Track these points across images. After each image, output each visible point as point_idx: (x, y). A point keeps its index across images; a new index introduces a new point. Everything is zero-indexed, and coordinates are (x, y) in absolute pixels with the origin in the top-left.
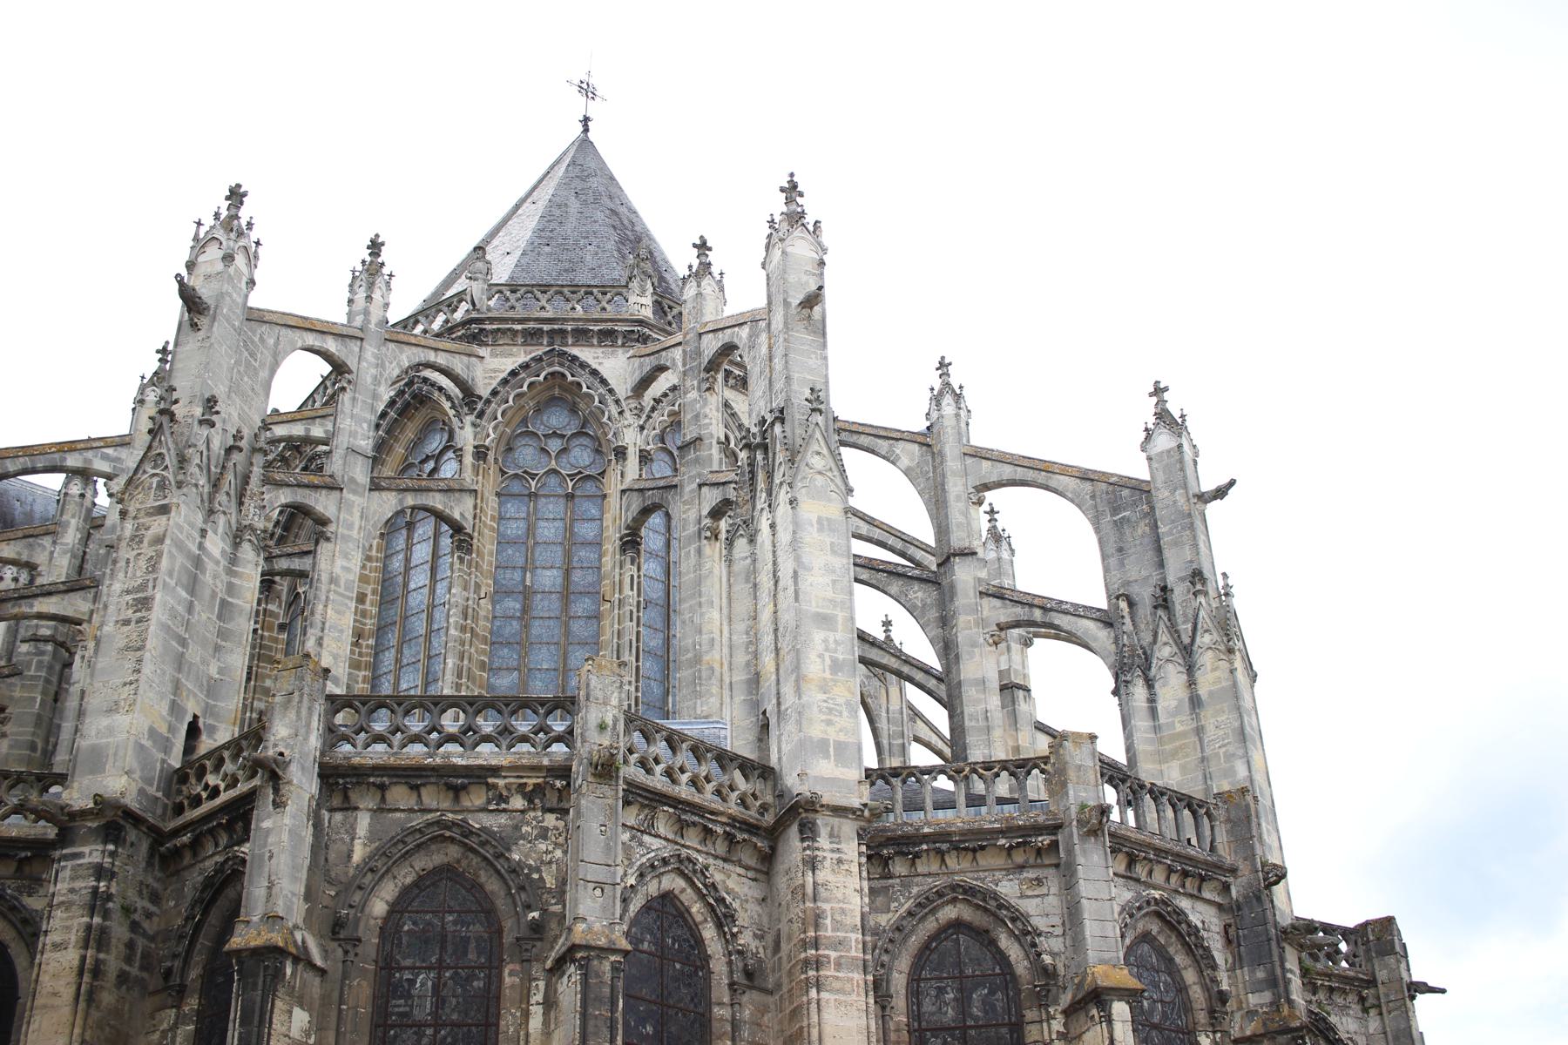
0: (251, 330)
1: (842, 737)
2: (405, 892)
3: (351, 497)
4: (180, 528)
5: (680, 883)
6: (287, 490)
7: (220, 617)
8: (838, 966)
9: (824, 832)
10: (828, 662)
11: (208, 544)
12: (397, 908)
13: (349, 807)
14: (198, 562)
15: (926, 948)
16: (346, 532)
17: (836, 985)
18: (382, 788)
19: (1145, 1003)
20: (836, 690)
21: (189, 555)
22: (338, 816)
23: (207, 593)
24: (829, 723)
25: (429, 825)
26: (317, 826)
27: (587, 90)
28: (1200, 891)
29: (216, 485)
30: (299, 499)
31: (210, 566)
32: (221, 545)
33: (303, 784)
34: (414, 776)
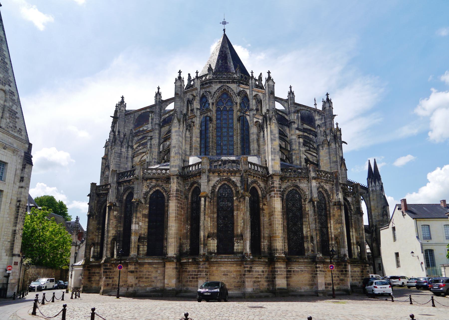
1: (176, 164)
2: (127, 196)
5: (158, 188)
8: (172, 197)
9: (172, 179)
11: (122, 150)
12: (127, 197)
14: (121, 154)
18: (123, 184)
21: (118, 153)
23: (123, 157)
24: (174, 162)
26: (118, 189)
27: (224, 23)
28: (235, 175)
29: (122, 142)
31: (123, 153)
33: (114, 186)
34: (125, 182)
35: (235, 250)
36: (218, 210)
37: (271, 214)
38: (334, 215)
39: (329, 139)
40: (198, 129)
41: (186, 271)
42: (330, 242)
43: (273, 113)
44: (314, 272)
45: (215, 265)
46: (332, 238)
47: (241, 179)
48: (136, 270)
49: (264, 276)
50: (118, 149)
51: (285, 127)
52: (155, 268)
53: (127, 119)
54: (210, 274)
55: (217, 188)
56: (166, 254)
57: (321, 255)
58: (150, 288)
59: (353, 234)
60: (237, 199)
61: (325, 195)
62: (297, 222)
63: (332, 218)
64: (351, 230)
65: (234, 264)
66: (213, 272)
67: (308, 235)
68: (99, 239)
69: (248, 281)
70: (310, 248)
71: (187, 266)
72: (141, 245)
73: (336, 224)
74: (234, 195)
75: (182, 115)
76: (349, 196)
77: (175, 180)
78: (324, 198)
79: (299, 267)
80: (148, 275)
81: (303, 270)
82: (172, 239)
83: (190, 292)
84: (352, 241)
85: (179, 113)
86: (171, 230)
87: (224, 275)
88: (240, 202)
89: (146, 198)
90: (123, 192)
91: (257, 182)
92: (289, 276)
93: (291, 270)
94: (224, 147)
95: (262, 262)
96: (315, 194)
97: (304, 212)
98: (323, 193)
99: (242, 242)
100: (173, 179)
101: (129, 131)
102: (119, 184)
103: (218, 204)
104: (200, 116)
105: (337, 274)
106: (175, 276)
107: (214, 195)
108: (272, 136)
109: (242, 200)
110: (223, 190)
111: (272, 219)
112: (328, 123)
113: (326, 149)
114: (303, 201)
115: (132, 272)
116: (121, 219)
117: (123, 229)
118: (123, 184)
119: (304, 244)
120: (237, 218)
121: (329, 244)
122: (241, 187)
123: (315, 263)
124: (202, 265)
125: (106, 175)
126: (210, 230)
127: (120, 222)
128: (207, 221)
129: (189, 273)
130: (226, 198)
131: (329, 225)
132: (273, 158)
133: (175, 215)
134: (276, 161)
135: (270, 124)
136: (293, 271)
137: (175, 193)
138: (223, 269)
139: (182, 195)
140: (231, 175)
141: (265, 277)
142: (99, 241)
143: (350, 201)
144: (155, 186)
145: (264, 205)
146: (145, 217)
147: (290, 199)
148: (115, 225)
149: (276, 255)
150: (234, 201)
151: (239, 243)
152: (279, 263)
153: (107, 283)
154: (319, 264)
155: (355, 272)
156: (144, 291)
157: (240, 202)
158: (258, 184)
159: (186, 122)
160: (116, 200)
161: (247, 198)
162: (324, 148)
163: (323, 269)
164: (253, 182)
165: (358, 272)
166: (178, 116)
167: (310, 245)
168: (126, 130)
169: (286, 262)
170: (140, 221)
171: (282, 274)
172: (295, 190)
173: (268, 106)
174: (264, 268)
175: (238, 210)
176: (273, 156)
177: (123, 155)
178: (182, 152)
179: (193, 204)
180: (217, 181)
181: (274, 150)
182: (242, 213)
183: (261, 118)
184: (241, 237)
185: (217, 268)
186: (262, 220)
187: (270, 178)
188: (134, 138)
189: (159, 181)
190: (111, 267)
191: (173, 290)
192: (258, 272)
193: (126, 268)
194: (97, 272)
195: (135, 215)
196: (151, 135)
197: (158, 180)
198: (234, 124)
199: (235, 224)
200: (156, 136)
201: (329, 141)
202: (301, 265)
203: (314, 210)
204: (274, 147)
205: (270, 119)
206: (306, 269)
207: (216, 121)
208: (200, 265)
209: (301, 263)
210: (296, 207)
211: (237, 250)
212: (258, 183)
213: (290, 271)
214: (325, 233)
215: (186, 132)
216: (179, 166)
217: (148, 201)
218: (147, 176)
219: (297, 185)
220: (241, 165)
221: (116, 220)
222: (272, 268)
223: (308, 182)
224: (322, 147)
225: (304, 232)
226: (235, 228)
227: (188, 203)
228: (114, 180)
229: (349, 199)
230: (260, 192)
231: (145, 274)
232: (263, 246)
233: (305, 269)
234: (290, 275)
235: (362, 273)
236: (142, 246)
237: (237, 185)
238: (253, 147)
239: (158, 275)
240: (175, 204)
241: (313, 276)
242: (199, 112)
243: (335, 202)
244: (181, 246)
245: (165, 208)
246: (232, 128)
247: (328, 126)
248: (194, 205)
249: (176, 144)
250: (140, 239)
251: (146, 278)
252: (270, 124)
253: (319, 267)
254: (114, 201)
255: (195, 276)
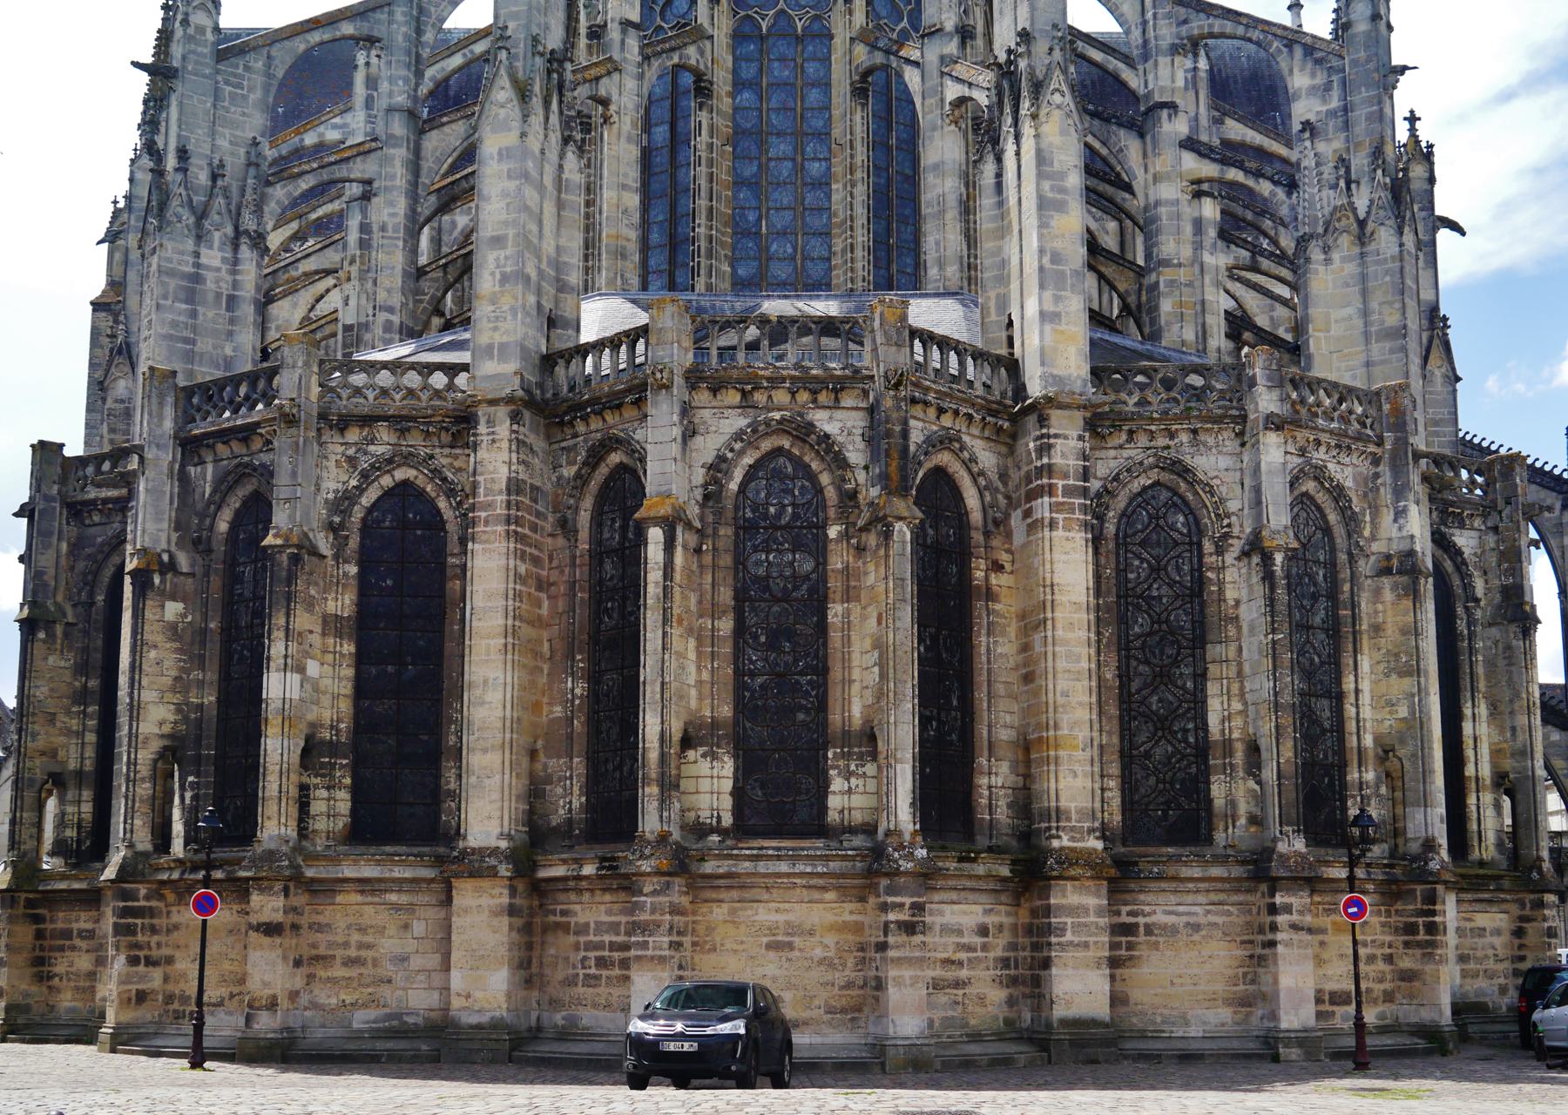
0: (232, 66)
1: (505, 339)
2: (238, 513)
3: (392, 151)
4: (169, 260)
6: (307, 177)
7: (228, 309)
8: (487, 523)
9: (483, 421)
10: (498, 276)
12: (235, 525)
13: (203, 463)
14: (196, 278)
15: (605, 487)
16: (389, 184)
17: (484, 537)
18: (212, 447)
19: (772, 510)
20: (503, 300)
21: (184, 276)
22: (199, 469)
23: (210, 297)
24: (495, 329)
25: (237, 466)
26: (183, 478)
28: (837, 400)
29: (201, 215)
30: (325, 177)
31: (209, 276)
32: (220, 255)
33: (163, 458)
34: (224, 435)
35: (833, 817)
36: (741, 597)
37: (1034, 621)
38: (1377, 629)
39: (1361, 204)
40: (629, 139)
41: (565, 928)
42: (1353, 775)
43: (1051, 49)
44: (1261, 931)
45: (723, 895)
46: (1361, 751)
47: (871, 428)
48: (291, 918)
49: (991, 955)
50: (182, 253)
51: (1122, 132)
52: (396, 907)
53: (227, 83)
54: (694, 944)
55: (738, 475)
56: (458, 834)
57: (1299, 845)
58: (372, 1017)
59: (1479, 729)
60: (845, 536)
61: (1333, 518)
62: (1176, 663)
63: (1365, 643)
64: (1468, 712)
65: (824, 889)
66: (710, 929)
67: (1235, 735)
68: (90, 752)
69: (899, 982)
70: (1243, 808)
71: (573, 897)
72: (316, 787)
73: (1387, 675)
74: (832, 513)
75: (538, 60)
76: (1462, 526)
77: (504, 429)
78: (1327, 530)
79: (1181, 909)
80: (361, 946)
81: (1202, 920)
82: (485, 751)
83: (588, 1036)
84: (1470, 770)
85: (520, 49)
86: (483, 703)
87: (769, 946)
88: (860, 550)
89: (342, 526)
90: (214, 491)
91: (959, 440)
92: (1123, 952)
93: (1136, 925)
94: (774, 247)
95: (979, 877)
96: (1276, 513)
97: (1211, 610)
98: (1319, 508)
99: (870, 769)
100: (490, 422)
101: (242, 151)
102: (190, 447)
103: (740, 562)
104: (640, 65)
105: (1382, 945)
106: (503, 951)
107: (719, 513)
108: (1046, 185)
109: (872, 539)
110: (769, 487)
111: (1038, 648)
112: (1360, 114)
113: (1344, 259)
114: (1208, 547)
115: (271, 929)
116: (203, 643)
117: (219, 700)
118: (212, 447)
119: (1208, 783)
120: (847, 641)
121: (1344, 785)
122: (866, 468)
123: (1264, 887)
124: (655, 893)
125: (116, 401)
126: (693, 704)
127: (202, 658)
128: (681, 656)
129: (582, 939)
130: (788, 527)
131: (1348, 684)
132: (1049, 307)
133: (501, 622)
134: (1063, 327)
135: (1034, 117)
136: (1147, 926)
137: (501, 499)
138: (765, 914)
139: (538, 514)
140: (815, 401)
141: (996, 959)
142: (89, 766)
143: (1467, 552)
144: (389, 463)
145: (998, 567)
146: (339, 634)
147: (1141, 536)
148: (174, 673)
149: (1056, 843)
150: (832, 546)
151: (858, 776)
152: (1069, 884)
153: (134, 987)
154: (1288, 891)
155: (1481, 931)
156: (340, 1032)
157: (860, 550)
158: (966, 455)
159: (561, 102)
160: (174, 536)
161: (903, 532)
162: (1336, 256)
163: (1308, 919)
164: (937, 442)
165: (1497, 932)
166: (519, 64)
167: (1243, 789)
168: (223, 143)
169: (1111, 880)
170: (307, 655)
171: (1086, 945)
172: (1168, 488)
173: (1023, 12)
174: (987, 912)
175: (849, 596)
176: (1048, 294)
177: (210, 285)
178: (540, 272)
179: (601, 563)
180: (738, 436)
181: (1053, 261)
182: (873, 612)
183: (986, 78)
184: (868, 741)
185: (733, 912)
186: (983, 650)
187: (1032, 420)
188: (270, 190)
189: (415, 433)
190: (154, 903)
191: (496, 1025)
192: (960, 932)
193: (236, 907)
194: (80, 932)
195: (282, 621)
196: (367, 176)
197: (408, 430)
198: (836, 113)
199: (836, 673)
200: (393, 177)
201: (1362, 215)
202: (1190, 898)
203: (1271, 602)
204: (1058, 245)
205: (1038, 87)
206: (1219, 920)
207: (733, 95)
208: (641, 893)
209: (1191, 885)
210: (1171, 584)
211: (842, 812)
212: (962, 449)
213: (1129, 929)
214: (1327, 725)
215: (562, 156)
216: (523, 348)
217: (354, 542)
218: (345, 404)
219: (1180, 461)
220: (868, 347)
221: (177, 651)
222: (1034, 913)
223: (1243, 445)
224: (1326, 250)
225: (1213, 720)
226: (835, 694)
227: (574, 557)
228: (160, 425)
229: (1465, 541)
230: (972, 500)
231: (340, 939)
232: (986, 793)
233: (1211, 918)
234: (1130, 947)
235: (1517, 942)
236: (324, 793)
237: (845, 459)
238: (937, 243)
239: (411, 946)
240: (504, 561)
241: (1251, 957)
242: (633, 43)
243: (1388, 557)
244: (535, 793)
245: (449, 585)
246: (824, 135)
247: (1360, 128)
248: (608, 566)
249: (506, 223)
250: (313, 755)
251: (349, 962)
252: (1034, 117)
253: (1288, 909)
254: (164, 546)
255: (616, 955)
